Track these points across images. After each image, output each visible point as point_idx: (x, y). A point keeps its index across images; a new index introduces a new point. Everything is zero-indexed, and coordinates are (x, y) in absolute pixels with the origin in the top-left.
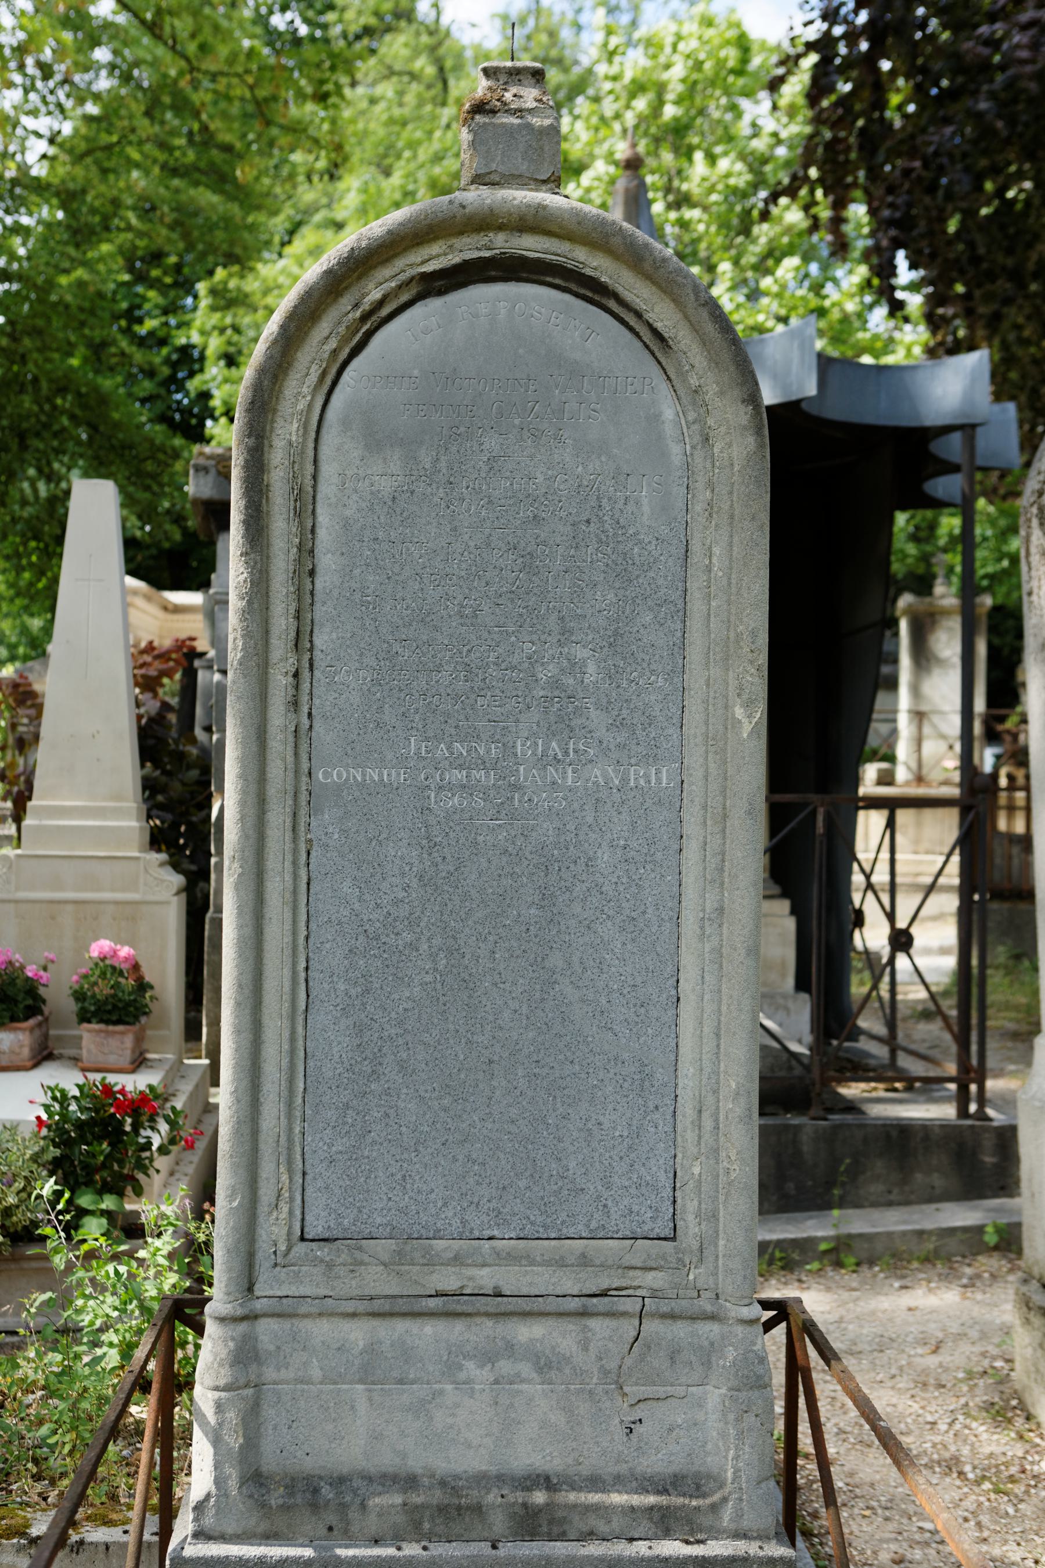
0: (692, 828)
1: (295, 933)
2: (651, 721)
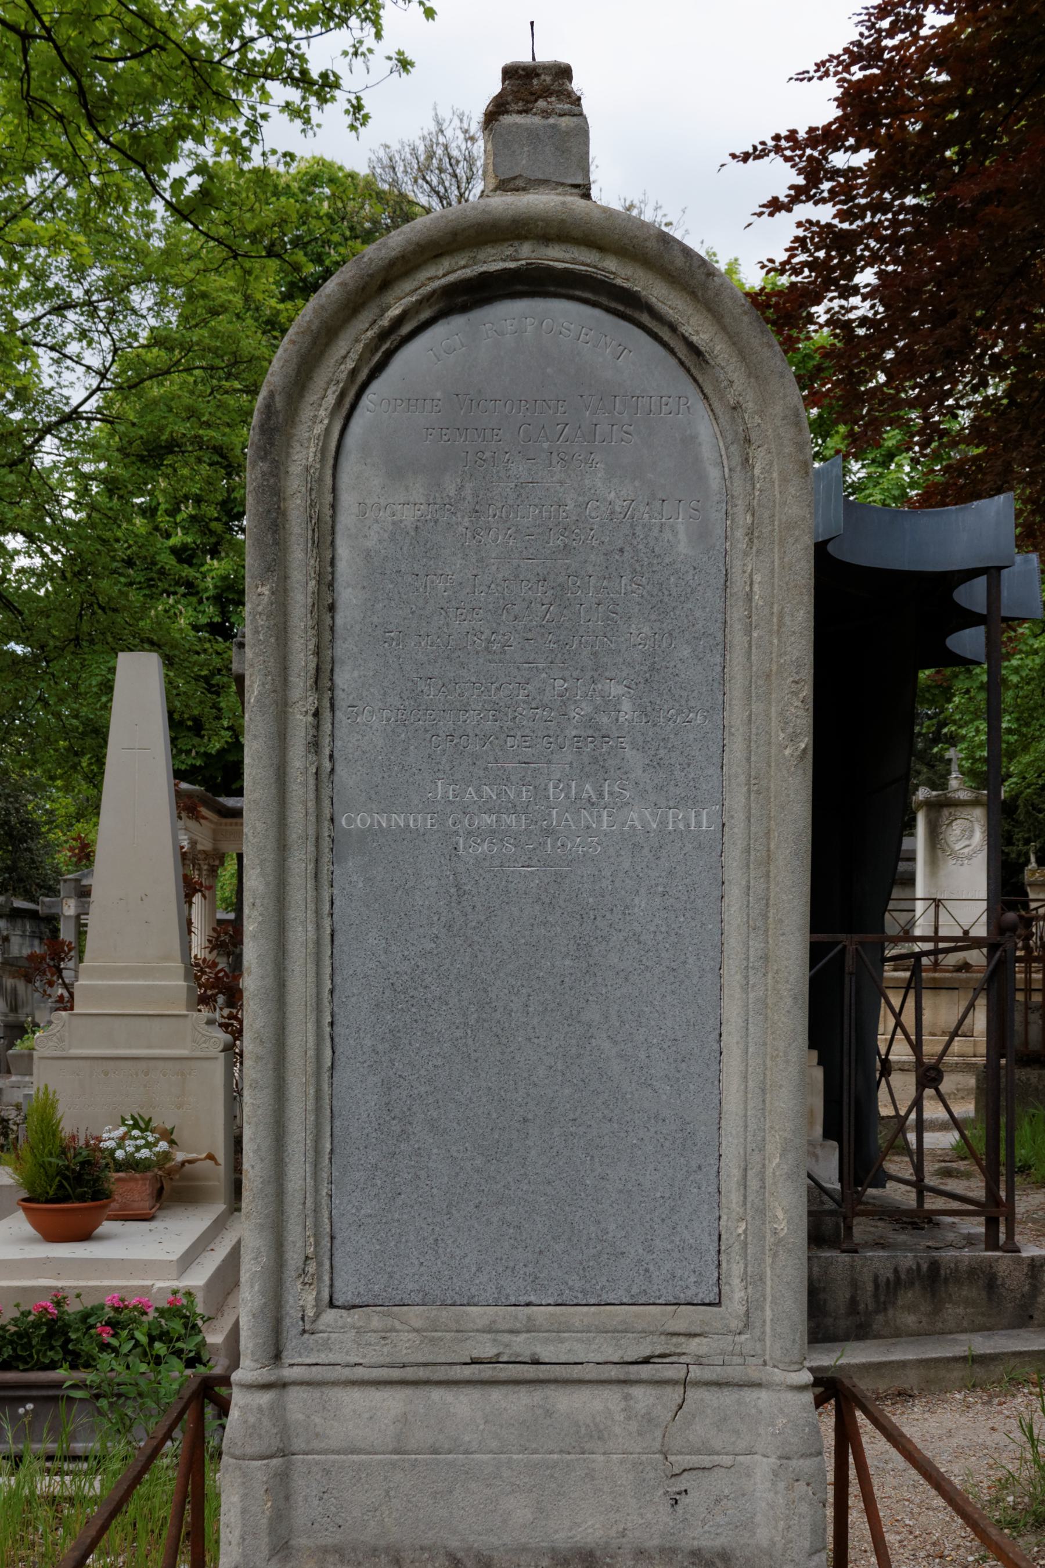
0: (734, 872)
1: (319, 984)
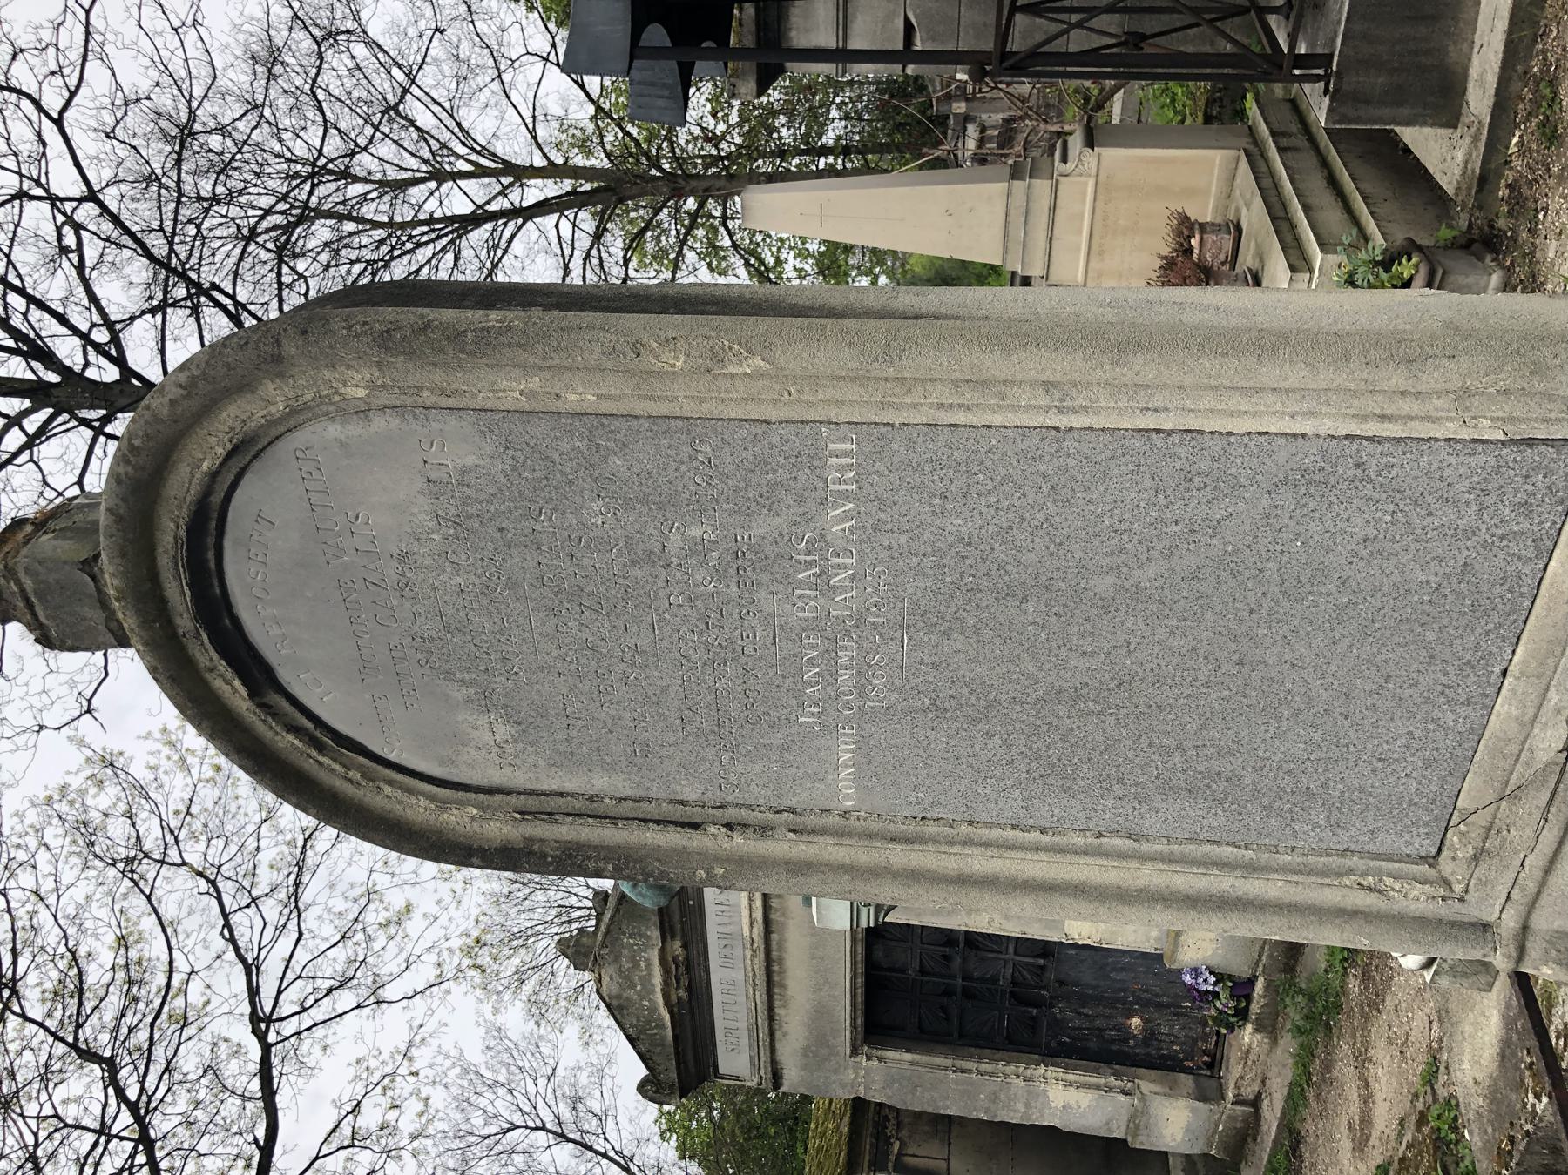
1: (1037, 849)
2: (762, 461)
